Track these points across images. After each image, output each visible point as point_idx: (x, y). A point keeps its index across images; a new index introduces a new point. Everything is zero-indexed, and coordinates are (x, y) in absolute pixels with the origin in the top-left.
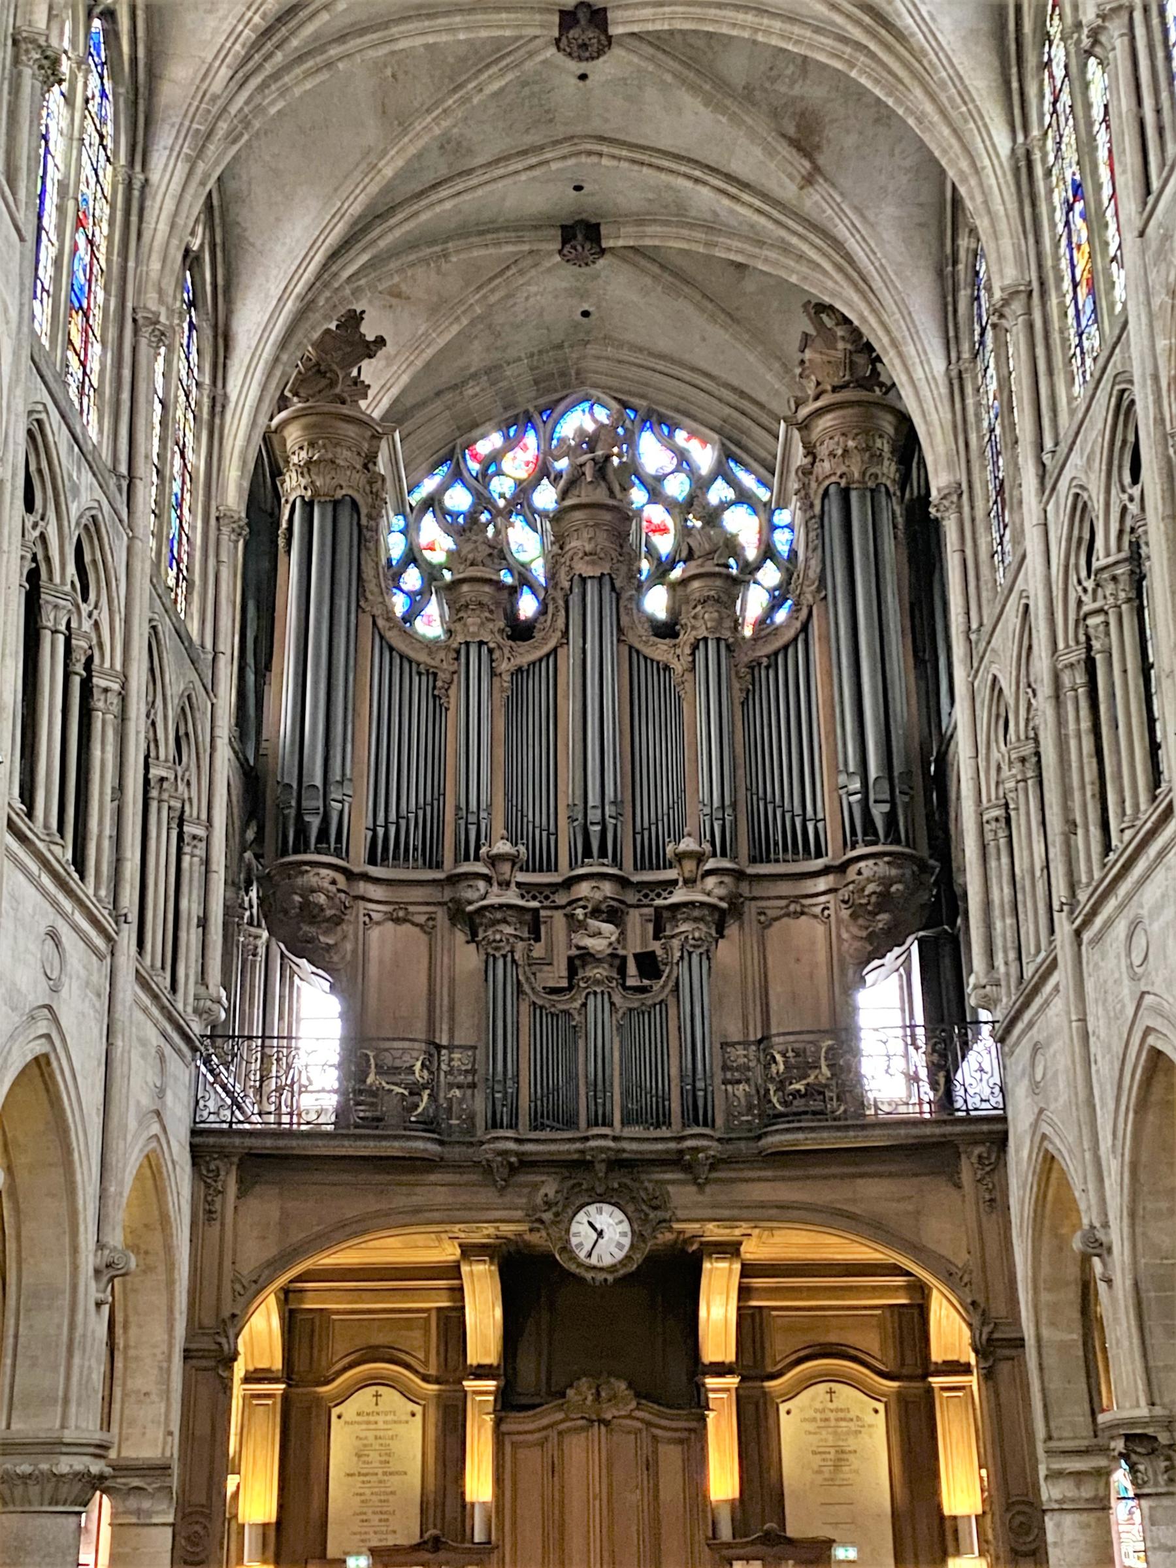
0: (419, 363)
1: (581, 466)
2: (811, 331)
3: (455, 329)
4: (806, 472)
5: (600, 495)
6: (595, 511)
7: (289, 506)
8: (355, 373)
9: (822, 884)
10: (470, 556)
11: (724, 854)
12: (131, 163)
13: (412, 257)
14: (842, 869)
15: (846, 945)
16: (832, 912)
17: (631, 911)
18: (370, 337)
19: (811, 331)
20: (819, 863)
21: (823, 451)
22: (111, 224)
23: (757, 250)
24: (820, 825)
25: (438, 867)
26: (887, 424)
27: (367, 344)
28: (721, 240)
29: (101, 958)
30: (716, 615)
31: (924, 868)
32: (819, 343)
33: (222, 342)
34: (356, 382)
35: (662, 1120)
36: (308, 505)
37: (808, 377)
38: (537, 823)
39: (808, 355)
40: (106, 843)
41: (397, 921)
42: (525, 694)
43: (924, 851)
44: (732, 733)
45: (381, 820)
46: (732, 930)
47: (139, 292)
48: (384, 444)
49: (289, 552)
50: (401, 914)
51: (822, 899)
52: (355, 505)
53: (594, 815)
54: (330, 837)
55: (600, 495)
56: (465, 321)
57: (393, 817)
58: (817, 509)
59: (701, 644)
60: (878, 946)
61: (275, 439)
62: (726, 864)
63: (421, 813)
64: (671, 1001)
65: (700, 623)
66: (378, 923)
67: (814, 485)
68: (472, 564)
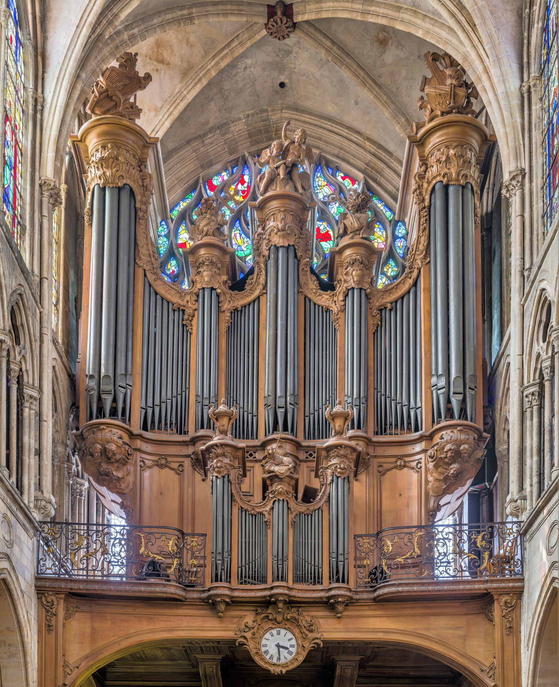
1: (277, 168)
2: (429, 75)
4: (421, 177)
5: (288, 189)
6: (287, 201)
7: (90, 193)
8: (132, 100)
9: (418, 448)
10: (205, 229)
11: (359, 427)
13: (169, 16)
14: (430, 437)
15: (430, 484)
16: (423, 465)
17: (302, 464)
18: (141, 74)
19: (429, 75)
20: (417, 434)
21: (432, 160)
23: (396, 14)
24: (418, 411)
25: (185, 433)
26: (475, 142)
27: (139, 79)
28: (373, 8)
30: (359, 272)
31: (480, 437)
32: (434, 81)
34: (133, 106)
35: (317, 580)
37: (425, 107)
38: (246, 409)
39: (427, 89)
41: (161, 466)
42: (237, 329)
43: (481, 426)
44: (367, 352)
45: (150, 403)
46: (363, 477)
48: (151, 153)
49: (91, 225)
50: (163, 462)
51: (418, 457)
52: (132, 193)
53: (281, 402)
54: (120, 412)
55: (288, 189)
57: (157, 402)
58: (427, 203)
59: (350, 293)
60: (449, 484)
61: (81, 145)
62: (360, 433)
63: (174, 399)
64: (325, 509)
65: (349, 277)
66: (149, 467)
67: (425, 185)
68: (206, 235)
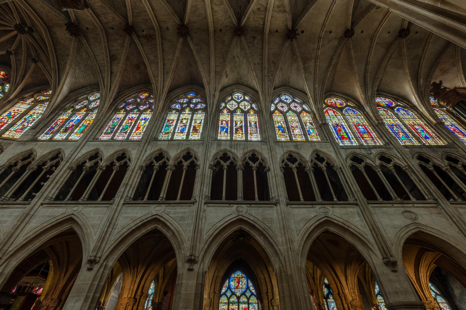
0: (462, 72)
3: (460, 63)
12: (364, 112)
18: (439, 83)
22: (366, 120)
29: (437, 207)
33: (414, 108)
36: (454, 109)
40: (424, 189)
47: (375, 123)
56: (460, 61)
